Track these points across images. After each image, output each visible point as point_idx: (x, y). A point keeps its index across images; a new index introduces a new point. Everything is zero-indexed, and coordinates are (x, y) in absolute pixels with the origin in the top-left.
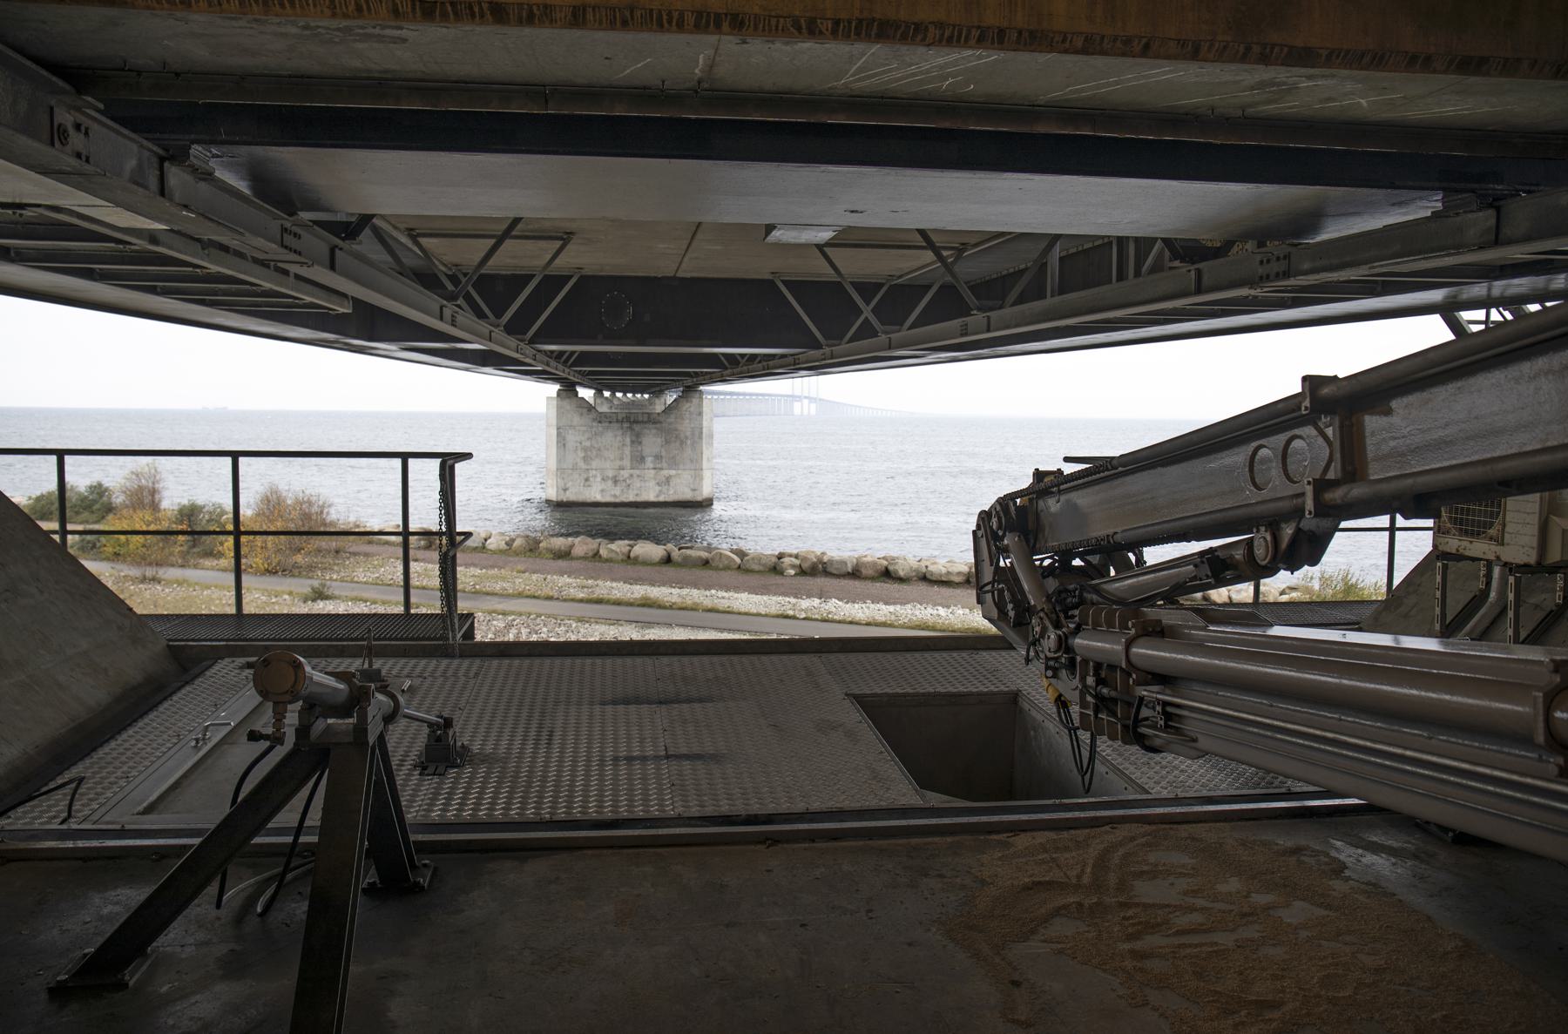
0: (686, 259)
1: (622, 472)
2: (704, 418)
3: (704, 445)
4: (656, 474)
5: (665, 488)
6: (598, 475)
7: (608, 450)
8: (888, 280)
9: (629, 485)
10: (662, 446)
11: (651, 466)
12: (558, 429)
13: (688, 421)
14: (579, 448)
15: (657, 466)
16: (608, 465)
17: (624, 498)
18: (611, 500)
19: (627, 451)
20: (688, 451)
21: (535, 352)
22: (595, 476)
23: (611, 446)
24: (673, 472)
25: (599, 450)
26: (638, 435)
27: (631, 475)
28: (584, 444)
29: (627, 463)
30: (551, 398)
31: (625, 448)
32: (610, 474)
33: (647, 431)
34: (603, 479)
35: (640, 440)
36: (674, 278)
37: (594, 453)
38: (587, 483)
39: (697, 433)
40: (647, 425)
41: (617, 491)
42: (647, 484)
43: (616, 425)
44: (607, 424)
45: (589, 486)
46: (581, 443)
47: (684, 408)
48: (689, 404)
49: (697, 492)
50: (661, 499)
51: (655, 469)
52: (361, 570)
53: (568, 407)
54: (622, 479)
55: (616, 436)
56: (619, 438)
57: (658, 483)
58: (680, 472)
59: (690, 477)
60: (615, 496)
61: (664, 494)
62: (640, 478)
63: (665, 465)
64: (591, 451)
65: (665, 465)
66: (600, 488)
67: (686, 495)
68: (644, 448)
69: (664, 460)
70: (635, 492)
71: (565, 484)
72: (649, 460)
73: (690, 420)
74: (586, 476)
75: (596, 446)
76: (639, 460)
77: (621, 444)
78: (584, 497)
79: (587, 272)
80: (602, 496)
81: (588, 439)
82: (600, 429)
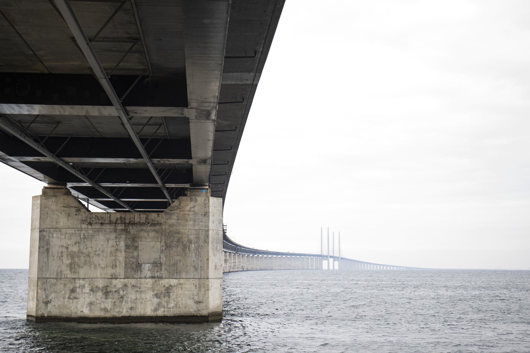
1: (114, 282)
2: (211, 218)
3: (210, 250)
4: (153, 284)
5: (164, 300)
6: (87, 285)
7: (99, 255)
9: (122, 297)
10: (162, 251)
11: (149, 274)
12: (40, 231)
13: (191, 223)
14: (65, 255)
15: (156, 275)
16: (98, 273)
17: (115, 313)
18: (102, 314)
19: (121, 257)
20: (192, 257)
22: (84, 286)
24: (174, 282)
25: (88, 256)
26: (134, 239)
27: (125, 285)
28: (70, 249)
29: (120, 271)
30: (36, 197)
31: (118, 254)
32: (101, 283)
34: (92, 290)
35: (136, 244)
38: (73, 295)
39: (202, 237)
40: (145, 228)
42: (143, 296)
43: (108, 227)
44: (98, 226)
45: (75, 298)
46: (67, 248)
47: (188, 208)
48: (192, 204)
49: (202, 306)
51: (153, 277)
53: (54, 207)
54: (114, 290)
56: (111, 242)
57: (156, 295)
58: (182, 281)
59: (193, 288)
60: (105, 310)
62: (136, 289)
63: (164, 273)
64: (79, 257)
65: (164, 273)
66: (88, 300)
68: (140, 254)
69: (163, 267)
70: (130, 305)
71: (47, 297)
72: (146, 267)
73: (194, 222)
74: (71, 287)
75: (84, 251)
77: (113, 249)
78: (69, 311)
80: (91, 310)
81: (76, 243)
82: (90, 232)
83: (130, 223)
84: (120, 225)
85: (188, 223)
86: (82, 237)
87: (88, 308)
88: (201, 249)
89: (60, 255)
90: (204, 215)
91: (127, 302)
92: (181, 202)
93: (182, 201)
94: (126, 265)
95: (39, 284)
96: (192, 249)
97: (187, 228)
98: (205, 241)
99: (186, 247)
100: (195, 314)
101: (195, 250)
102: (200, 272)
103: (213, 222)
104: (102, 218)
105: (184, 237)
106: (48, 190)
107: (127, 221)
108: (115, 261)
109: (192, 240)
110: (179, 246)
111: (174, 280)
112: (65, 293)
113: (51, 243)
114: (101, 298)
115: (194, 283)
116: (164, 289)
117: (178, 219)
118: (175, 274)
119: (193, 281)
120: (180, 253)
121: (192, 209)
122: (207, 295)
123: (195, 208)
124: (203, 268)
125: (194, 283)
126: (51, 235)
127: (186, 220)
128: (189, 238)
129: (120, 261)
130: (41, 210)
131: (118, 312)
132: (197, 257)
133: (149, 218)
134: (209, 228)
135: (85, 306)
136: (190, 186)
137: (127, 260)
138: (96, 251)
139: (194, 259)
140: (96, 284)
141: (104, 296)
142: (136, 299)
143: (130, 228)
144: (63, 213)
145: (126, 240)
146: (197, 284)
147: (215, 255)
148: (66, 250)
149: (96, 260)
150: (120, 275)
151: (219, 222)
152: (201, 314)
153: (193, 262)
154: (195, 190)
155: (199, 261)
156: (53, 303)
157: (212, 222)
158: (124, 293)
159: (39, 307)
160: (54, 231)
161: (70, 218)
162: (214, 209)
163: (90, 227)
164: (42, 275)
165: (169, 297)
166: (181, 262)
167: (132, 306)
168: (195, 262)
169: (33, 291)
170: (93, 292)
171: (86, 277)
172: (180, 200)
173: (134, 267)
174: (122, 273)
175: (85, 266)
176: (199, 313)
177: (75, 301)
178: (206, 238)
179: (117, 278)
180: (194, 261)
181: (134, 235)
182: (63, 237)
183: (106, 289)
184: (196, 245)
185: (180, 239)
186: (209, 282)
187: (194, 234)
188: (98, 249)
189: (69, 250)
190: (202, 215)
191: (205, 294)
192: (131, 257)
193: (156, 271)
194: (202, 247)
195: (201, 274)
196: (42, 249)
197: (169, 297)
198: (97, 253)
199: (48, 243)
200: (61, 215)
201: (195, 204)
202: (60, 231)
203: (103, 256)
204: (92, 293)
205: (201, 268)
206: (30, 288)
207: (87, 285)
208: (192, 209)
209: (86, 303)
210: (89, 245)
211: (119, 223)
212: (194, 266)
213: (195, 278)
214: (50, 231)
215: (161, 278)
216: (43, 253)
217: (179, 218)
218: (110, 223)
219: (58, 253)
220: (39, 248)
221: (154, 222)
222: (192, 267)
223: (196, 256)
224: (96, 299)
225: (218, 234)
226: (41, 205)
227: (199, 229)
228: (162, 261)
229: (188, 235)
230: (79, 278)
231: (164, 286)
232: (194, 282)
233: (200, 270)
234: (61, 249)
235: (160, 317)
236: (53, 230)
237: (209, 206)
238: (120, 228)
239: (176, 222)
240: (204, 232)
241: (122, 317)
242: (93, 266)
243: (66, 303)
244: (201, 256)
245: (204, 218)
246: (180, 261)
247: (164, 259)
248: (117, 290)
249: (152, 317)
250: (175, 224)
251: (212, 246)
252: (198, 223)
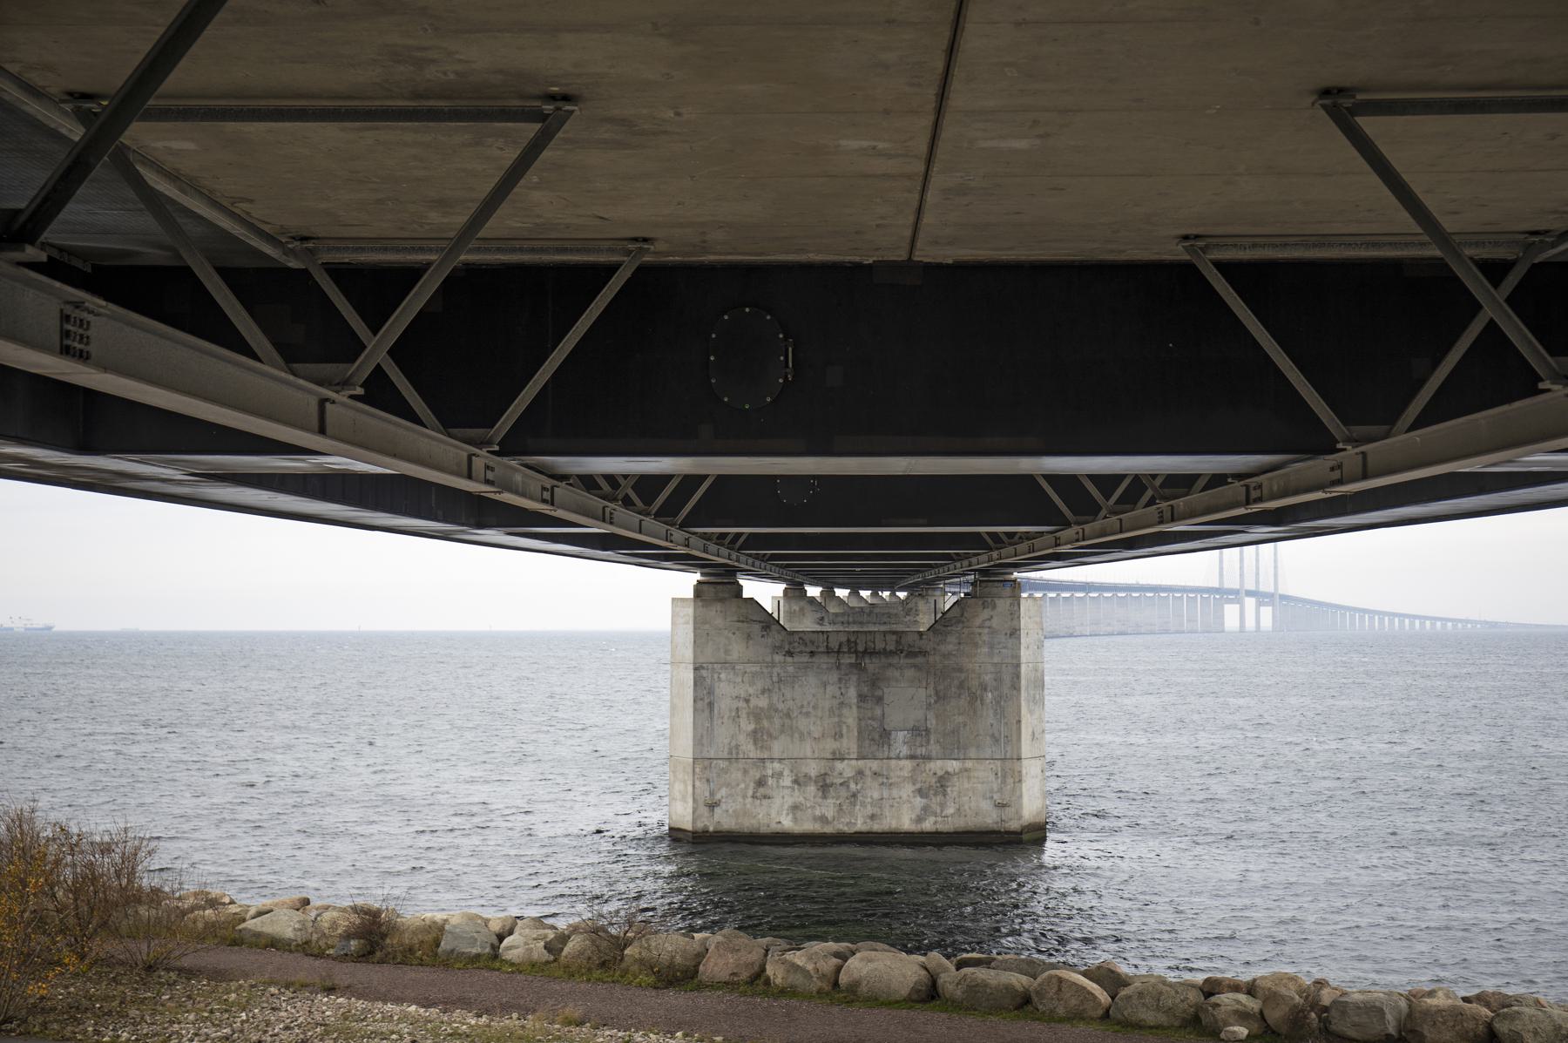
0: (931, 197)
1: (839, 765)
3: (1023, 703)
4: (914, 770)
6: (786, 773)
7: (807, 714)
8: (1529, 247)
9: (854, 796)
10: (929, 706)
11: (905, 751)
12: (696, 669)
13: (985, 650)
14: (743, 714)
15: (919, 752)
16: (807, 749)
17: (842, 826)
18: (816, 828)
19: (851, 717)
20: (988, 718)
21: (548, 483)
22: (781, 774)
23: (815, 708)
24: (952, 766)
25: (788, 715)
26: (874, 683)
27: (860, 773)
28: (754, 702)
29: (850, 744)
30: (683, 600)
31: (845, 711)
32: (813, 769)
33: (890, 673)
34: (796, 782)
35: (879, 693)
36: (909, 266)
37: (777, 722)
38: (762, 791)
39: (1007, 678)
40: (894, 660)
41: (828, 809)
42: (895, 793)
43: (824, 661)
44: (805, 658)
45: (766, 797)
46: (747, 701)
47: (978, 621)
48: (986, 613)
49: (1009, 812)
50: (928, 825)
51: (912, 757)
52: (192, 1017)
53: (719, 622)
55: (825, 685)
58: (969, 764)
59: (992, 777)
60: (823, 819)
61: (936, 815)
62: (880, 780)
63: (934, 749)
64: (770, 718)
65: (934, 749)
66: (789, 801)
67: (983, 815)
69: (933, 738)
70: (869, 810)
72: (901, 736)
73: (992, 647)
74: (758, 776)
75: (780, 706)
76: (877, 738)
77: (835, 702)
78: (754, 822)
79: (664, 251)
80: (795, 820)
81: (763, 692)
82: (791, 669)
83: (865, 652)
84: (846, 655)
86: (775, 679)
87: (791, 816)
89: (733, 714)
91: (863, 805)
94: (859, 732)
95: (697, 770)
100: (995, 827)
104: (812, 642)
106: (705, 587)
107: (861, 648)
108: (840, 726)
111: (954, 762)
112: (747, 788)
113: (717, 691)
114: (815, 797)
116: (934, 780)
121: (987, 624)
122: (1018, 793)
126: (716, 676)
127: (976, 645)
129: (848, 726)
130: (695, 629)
131: (847, 824)
133: (903, 641)
134: (1019, 660)
135: (785, 812)
137: (863, 723)
138: (802, 706)
140: (805, 770)
141: (820, 794)
142: (882, 799)
143: (867, 661)
144: (737, 633)
145: (858, 685)
147: (1031, 712)
148: (745, 705)
149: (802, 723)
150: (848, 753)
154: (990, 584)
156: (724, 806)
158: (859, 787)
159: (698, 812)
160: (721, 668)
161: (751, 642)
163: (789, 659)
164: (701, 752)
165: (944, 796)
166: (968, 727)
167: (875, 812)
169: (685, 782)
170: (799, 784)
171: (785, 756)
173: (877, 737)
174: (854, 748)
175: (783, 736)
177: (765, 802)
179: (844, 759)
181: (874, 674)
182: (739, 679)
183: (824, 780)
185: (963, 681)
186: (1021, 767)
188: (805, 703)
189: (751, 706)
191: (1013, 790)
192: (869, 719)
193: (917, 744)
196: (700, 704)
197: (944, 796)
198: (804, 710)
199: (711, 692)
200: (734, 637)
201: (992, 613)
202: (733, 668)
203: (816, 716)
204: (796, 787)
206: (675, 776)
207: (786, 773)
208: (987, 624)
209: (786, 807)
210: (788, 695)
211: (844, 652)
212: (993, 736)
214: (713, 669)
215: (928, 758)
216: (703, 711)
218: (828, 652)
219: (730, 711)
220: (695, 701)
221: (912, 649)
222: (988, 738)
224: (805, 798)
226: (695, 618)
228: (929, 726)
229: (980, 674)
230: (772, 760)
231: (935, 774)
234: (736, 704)
235: (927, 833)
236: (720, 666)
237: (1019, 617)
238: (848, 661)
241: (856, 833)
242: (796, 735)
243: (748, 806)
246: (965, 725)
247: (934, 722)
248: (845, 782)
249: (913, 833)
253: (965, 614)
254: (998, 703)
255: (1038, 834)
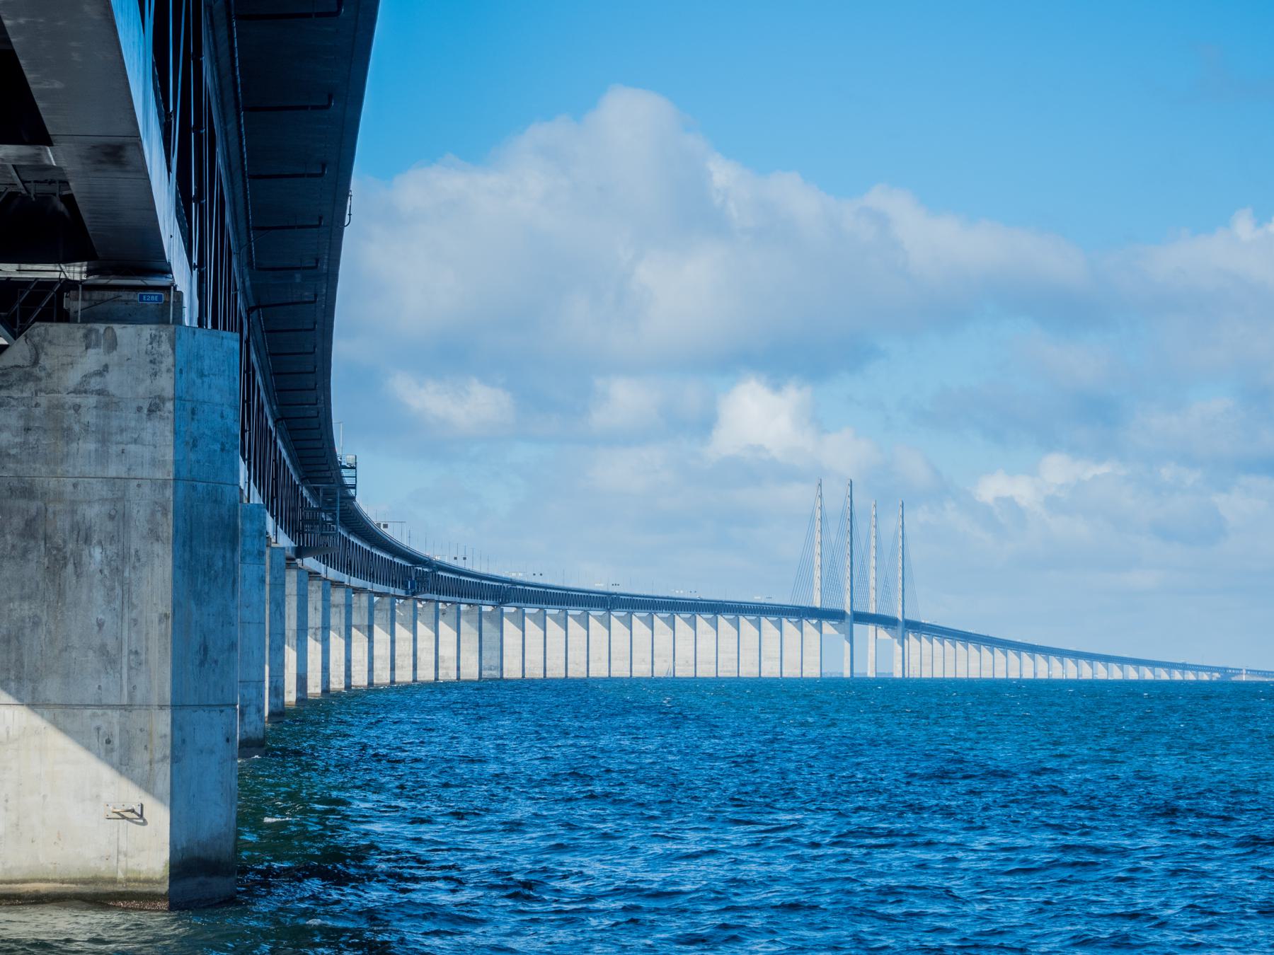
48: (92, 359)
73: (104, 439)
85: (74, 445)
88: (134, 567)
90: (150, 411)
92: (43, 348)
93: (46, 344)
96: (93, 567)
97: (70, 469)
98: (151, 530)
99: (65, 558)
101: (106, 572)
102: (129, 678)
103: (195, 445)
105: (54, 513)
109: (90, 528)
110: (30, 557)
115: (98, 729)
117: (27, 430)
118: (12, 684)
119: (94, 715)
120: (38, 587)
121: (95, 383)
123: (108, 376)
124: (143, 657)
125: (98, 729)
128: (78, 517)
132: (117, 604)
136: (89, 272)
139: (100, 616)
146: (116, 730)
151: (223, 444)
152: (133, 871)
153: (96, 628)
155: (126, 626)
157: (187, 443)
162: (198, 381)
166: (42, 631)
168: (104, 628)
172: (36, 339)
176: (122, 864)
178: (159, 515)
180: (100, 625)
184: (112, 550)
185: (34, 519)
187: (103, 500)
190: (139, 409)
194: (139, 560)
195: (134, 687)
205: (132, 657)
212: (103, 650)
213: (104, 702)
217: (31, 424)
222: (91, 654)
223: (109, 602)
225: (216, 501)
227: (123, 476)
229: (73, 502)
232: (98, 722)
233: (130, 668)
239: (18, 440)
240: (146, 489)
244: (135, 601)
245: (149, 424)
246: (36, 624)
250: (13, 452)
251: (187, 556)
252: (121, 447)
253: (43, 360)
254: (117, 571)
255: (190, 884)
